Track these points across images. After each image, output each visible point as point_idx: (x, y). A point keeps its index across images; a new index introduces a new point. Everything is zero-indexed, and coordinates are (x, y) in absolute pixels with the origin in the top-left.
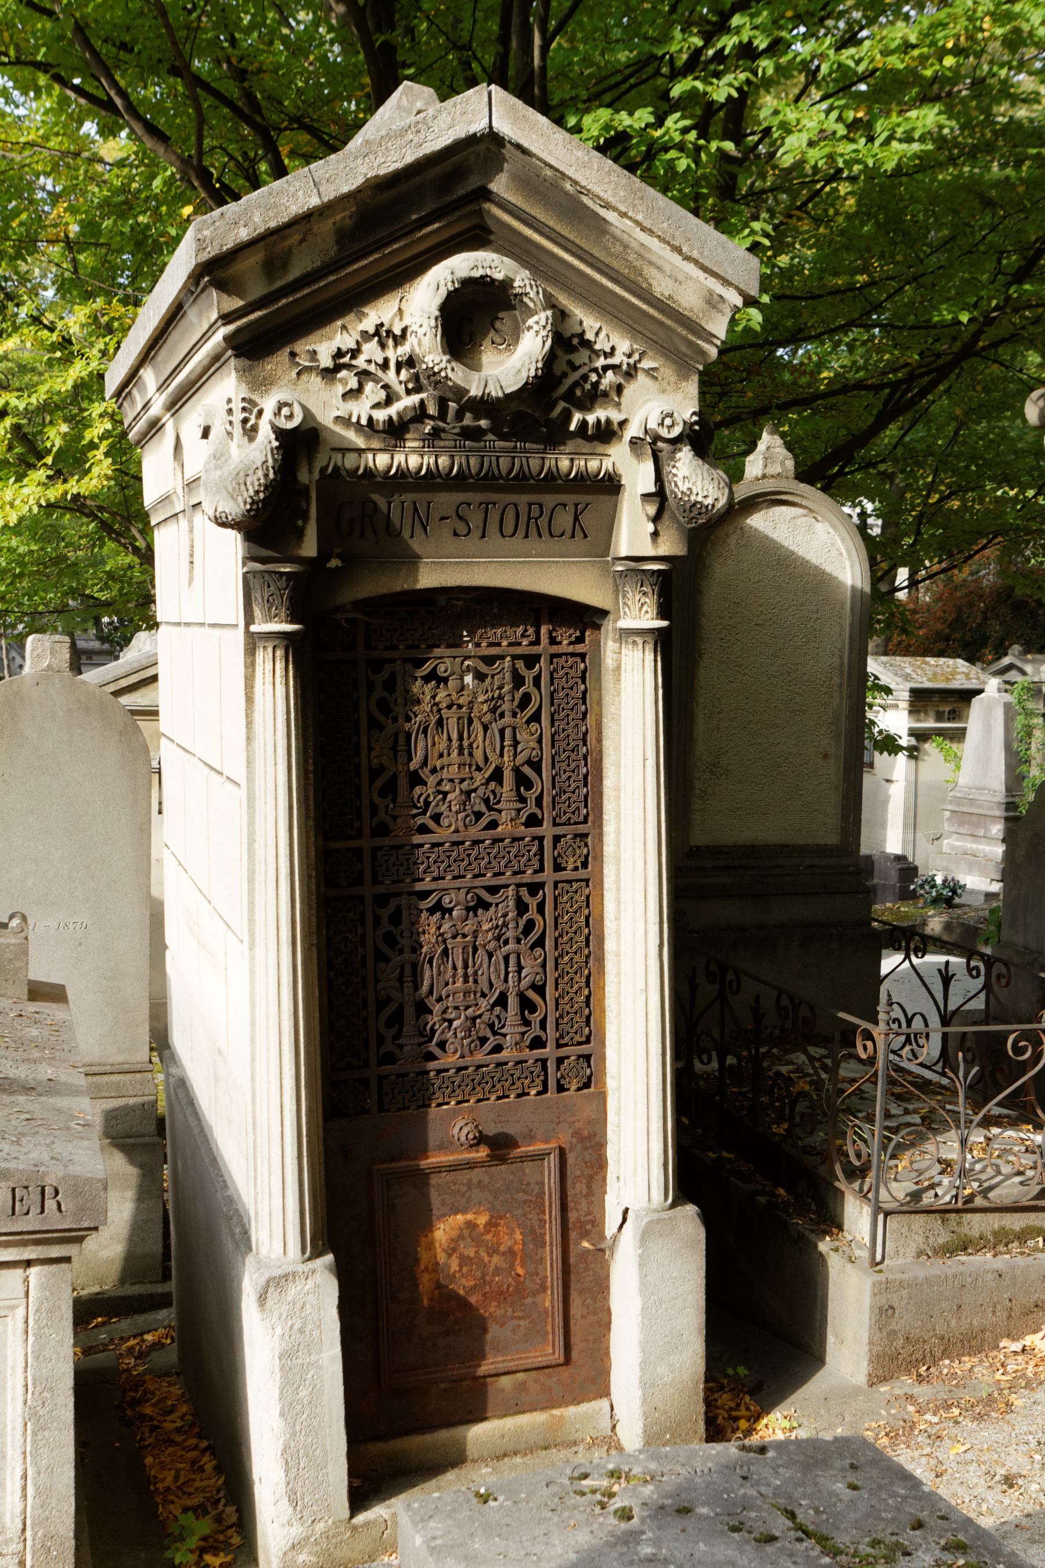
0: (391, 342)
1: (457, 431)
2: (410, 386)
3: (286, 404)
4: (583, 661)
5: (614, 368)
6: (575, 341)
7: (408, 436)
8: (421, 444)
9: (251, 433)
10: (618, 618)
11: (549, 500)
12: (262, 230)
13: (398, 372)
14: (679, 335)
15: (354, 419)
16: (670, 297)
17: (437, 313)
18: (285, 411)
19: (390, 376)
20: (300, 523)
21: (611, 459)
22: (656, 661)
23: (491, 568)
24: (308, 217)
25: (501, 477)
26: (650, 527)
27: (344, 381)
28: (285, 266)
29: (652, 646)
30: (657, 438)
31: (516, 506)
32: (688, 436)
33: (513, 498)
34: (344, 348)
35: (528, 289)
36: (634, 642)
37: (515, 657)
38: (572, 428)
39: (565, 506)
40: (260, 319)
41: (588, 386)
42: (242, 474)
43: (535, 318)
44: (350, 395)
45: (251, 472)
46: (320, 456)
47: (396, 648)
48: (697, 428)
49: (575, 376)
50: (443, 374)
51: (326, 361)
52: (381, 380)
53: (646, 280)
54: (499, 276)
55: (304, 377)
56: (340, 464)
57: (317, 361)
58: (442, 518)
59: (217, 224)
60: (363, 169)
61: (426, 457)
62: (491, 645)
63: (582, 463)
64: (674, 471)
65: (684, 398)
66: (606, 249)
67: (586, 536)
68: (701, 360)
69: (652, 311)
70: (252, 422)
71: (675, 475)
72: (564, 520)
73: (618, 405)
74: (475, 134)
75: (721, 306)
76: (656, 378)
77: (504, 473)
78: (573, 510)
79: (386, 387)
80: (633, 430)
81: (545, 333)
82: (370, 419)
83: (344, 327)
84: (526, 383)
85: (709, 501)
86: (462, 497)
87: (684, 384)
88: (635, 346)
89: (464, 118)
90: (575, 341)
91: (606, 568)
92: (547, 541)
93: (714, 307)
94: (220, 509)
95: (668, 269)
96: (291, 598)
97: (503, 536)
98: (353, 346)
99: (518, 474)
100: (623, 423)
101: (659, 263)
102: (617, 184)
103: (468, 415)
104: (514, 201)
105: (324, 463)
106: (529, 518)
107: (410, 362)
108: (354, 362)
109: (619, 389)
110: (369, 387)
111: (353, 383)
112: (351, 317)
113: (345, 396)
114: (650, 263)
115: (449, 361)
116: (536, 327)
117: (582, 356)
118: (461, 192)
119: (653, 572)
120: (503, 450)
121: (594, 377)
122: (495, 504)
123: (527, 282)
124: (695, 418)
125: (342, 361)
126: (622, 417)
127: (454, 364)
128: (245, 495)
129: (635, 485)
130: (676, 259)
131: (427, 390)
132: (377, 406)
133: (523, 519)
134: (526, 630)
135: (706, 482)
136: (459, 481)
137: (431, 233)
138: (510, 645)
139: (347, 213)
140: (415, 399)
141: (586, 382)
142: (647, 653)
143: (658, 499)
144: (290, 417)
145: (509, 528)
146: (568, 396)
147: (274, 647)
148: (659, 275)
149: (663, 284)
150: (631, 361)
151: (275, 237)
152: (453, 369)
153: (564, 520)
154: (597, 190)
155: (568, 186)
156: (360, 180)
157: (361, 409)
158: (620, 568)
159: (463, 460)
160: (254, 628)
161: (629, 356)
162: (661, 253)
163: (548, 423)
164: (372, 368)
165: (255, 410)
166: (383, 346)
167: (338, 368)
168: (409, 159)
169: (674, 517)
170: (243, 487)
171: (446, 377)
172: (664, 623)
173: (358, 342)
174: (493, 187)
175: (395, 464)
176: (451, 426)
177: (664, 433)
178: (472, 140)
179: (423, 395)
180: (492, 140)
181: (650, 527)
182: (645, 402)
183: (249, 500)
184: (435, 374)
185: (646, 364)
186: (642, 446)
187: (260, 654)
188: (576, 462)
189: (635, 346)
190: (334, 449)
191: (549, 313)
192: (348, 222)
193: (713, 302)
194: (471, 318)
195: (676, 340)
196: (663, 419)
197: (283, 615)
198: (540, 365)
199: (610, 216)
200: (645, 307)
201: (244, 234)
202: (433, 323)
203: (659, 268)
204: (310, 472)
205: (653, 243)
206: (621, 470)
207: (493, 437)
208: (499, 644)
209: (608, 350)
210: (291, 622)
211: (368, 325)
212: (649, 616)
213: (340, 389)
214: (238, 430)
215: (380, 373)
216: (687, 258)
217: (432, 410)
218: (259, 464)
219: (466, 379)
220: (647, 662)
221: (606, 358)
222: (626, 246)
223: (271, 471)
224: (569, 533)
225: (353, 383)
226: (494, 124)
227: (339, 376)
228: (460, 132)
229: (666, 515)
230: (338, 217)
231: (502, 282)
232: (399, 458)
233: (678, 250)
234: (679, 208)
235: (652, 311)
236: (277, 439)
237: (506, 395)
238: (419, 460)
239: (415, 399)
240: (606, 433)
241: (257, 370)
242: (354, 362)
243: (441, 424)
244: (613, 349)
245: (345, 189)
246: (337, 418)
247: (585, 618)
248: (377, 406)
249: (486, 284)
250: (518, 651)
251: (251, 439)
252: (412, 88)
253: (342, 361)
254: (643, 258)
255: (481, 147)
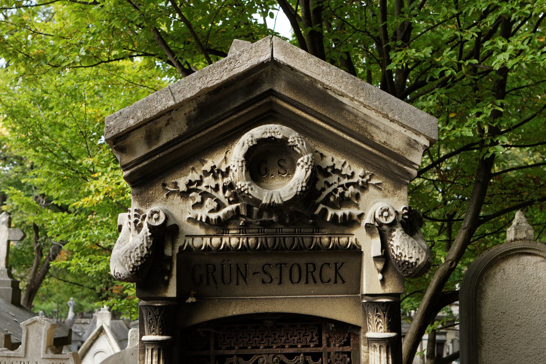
0: (220, 176)
1: (258, 223)
2: (231, 199)
3: (156, 212)
4: (349, 356)
5: (355, 185)
6: (329, 170)
7: (230, 227)
8: (238, 231)
9: (139, 228)
10: (367, 331)
11: (319, 261)
12: (142, 120)
13: (224, 192)
14: (393, 164)
15: (199, 219)
16: (385, 143)
17: (243, 159)
18: (155, 216)
19: (220, 195)
20: (166, 278)
21: (354, 237)
22: (388, 358)
23: (286, 302)
24: (169, 111)
25: (286, 248)
26: (380, 276)
27: (193, 198)
28: (158, 138)
29: (385, 348)
30: (381, 224)
31: (299, 265)
32: (401, 222)
33: (297, 260)
34: (193, 180)
35: (297, 143)
36: (375, 346)
37: (306, 354)
38: (328, 219)
39: (329, 264)
40: (147, 165)
41: (337, 195)
42: (129, 251)
43: (301, 159)
44: (198, 205)
45: (133, 250)
46: (179, 240)
47: (234, 348)
48: (407, 217)
49: (330, 190)
50: (246, 192)
51: (182, 187)
52: (215, 197)
53: (370, 134)
54: (279, 137)
55: (171, 197)
56: (191, 243)
57: (178, 188)
58: (254, 273)
59: (118, 118)
60: (199, 85)
61: (241, 239)
62: (291, 347)
63: (336, 239)
64: (391, 243)
65: (399, 200)
66: (344, 118)
67: (344, 282)
68: (407, 177)
69: (374, 151)
70: (139, 222)
71: (392, 245)
72: (329, 272)
73: (357, 206)
74: (263, 62)
75: (416, 146)
76: (380, 189)
77: (288, 246)
78: (334, 267)
79: (217, 200)
80: (368, 219)
81: (307, 167)
82: (208, 218)
83: (193, 169)
84: (296, 195)
85: (413, 260)
86: (265, 261)
87: (398, 192)
88: (367, 172)
89: (257, 54)
90: (329, 170)
91: (358, 301)
92: (321, 287)
93: (413, 147)
94: (116, 272)
95: (382, 127)
96: (162, 321)
97: (292, 282)
98: (198, 178)
99: (297, 247)
100: (361, 216)
101: (377, 124)
102: (347, 83)
103: (265, 214)
104: (289, 96)
105: (181, 244)
106: (307, 272)
107: (231, 186)
108: (199, 188)
109: (357, 196)
110: (208, 201)
111: (198, 199)
112: (198, 163)
113: (195, 206)
114: (372, 125)
115: (249, 185)
116: (302, 164)
117: (334, 178)
118: (258, 93)
119: (383, 303)
120: (287, 233)
121: (340, 190)
122: (285, 264)
123: (296, 139)
124: (405, 211)
125: (192, 187)
126: (360, 212)
127: (253, 186)
128: (130, 263)
129: (370, 251)
130: (386, 122)
131: (241, 201)
132: (212, 211)
133: (304, 273)
134: (313, 338)
135: (411, 249)
136: (263, 250)
137: (242, 116)
138: (303, 347)
139: (192, 108)
140: (234, 206)
141: (336, 193)
142: (382, 353)
143: (384, 259)
144: (157, 219)
145: (296, 277)
146: (326, 201)
147: (152, 350)
148: (377, 131)
149: (380, 136)
150: (365, 180)
151: (151, 123)
152: (252, 189)
153: (329, 272)
154: (336, 87)
155: (319, 86)
156: (198, 90)
157: (203, 213)
158: (364, 301)
159: (264, 240)
160: (144, 338)
161: (363, 177)
162: (377, 119)
163: (313, 217)
164: (209, 190)
165: (141, 216)
166: (215, 178)
167: (189, 191)
168: (225, 78)
169: (395, 270)
170: (128, 259)
171: (248, 194)
172: (393, 334)
173: (201, 177)
174: (277, 89)
175: (223, 243)
176: (254, 220)
177: (383, 220)
178: (262, 65)
179: (239, 204)
180: (273, 63)
181: (380, 276)
182: (374, 203)
183: (132, 266)
184: (242, 192)
185: (374, 181)
186: (373, 228)
187: (148, 353)
188: (315, 240)
189: (367, 172)
190: (187, 236)
191: (310, 155)
192: (193, 113)
193: (412, 145)
194: (264, 161)
195: (391, 166)
196: (382, 213)
197: (157, 330)
198: (304, 184)
199: (345, 100)
200: (370, 149)
201: (132, 122)
202: (240, 164)
203: (377, 127)
204: (173, 249)
205: (372, 114)
206: (361, 243)
207: (281, 226)
208: (296, 347)
209: (350, 174)
210: (162, 335)
211: (207, 167)
212: (382, 330)
213: (191, 203)
214: (133, 227)
215: (214, 193)
216: (392, 121)
217: (243, 212)
218: (138, 246)
219: (260, 194)
220: (382, 359)
221: (348, 179)
222: (356, 116)
223: (145, 249)
224: (333, 280)
225: (198, 199)
226: (274, 56)
227: (191, 195)
228: (255, 61)
229: (390, 270)
230: (187, 111)
231: (282, 139)
232: (226, 240)
233: (386, 116)
234: (385, 93)
235: (374, 151)
236: (150, 231)
237: (285, 202)
238: (238, 240)
239: (234, 206)
240: (350, 222)
241: (144, 195)
242: (199, 188)
243: (249, 220)
244: (353, 173)
245: (189, 96)
246: (189, 219)
247: (349, 333)
248: (212, 211)
249: (272, 141)
250: (308, 350)
251: (139, 232)
252: (238, 42)
253: (192, 187)
254: (367, 122)
255: (269, 68)
